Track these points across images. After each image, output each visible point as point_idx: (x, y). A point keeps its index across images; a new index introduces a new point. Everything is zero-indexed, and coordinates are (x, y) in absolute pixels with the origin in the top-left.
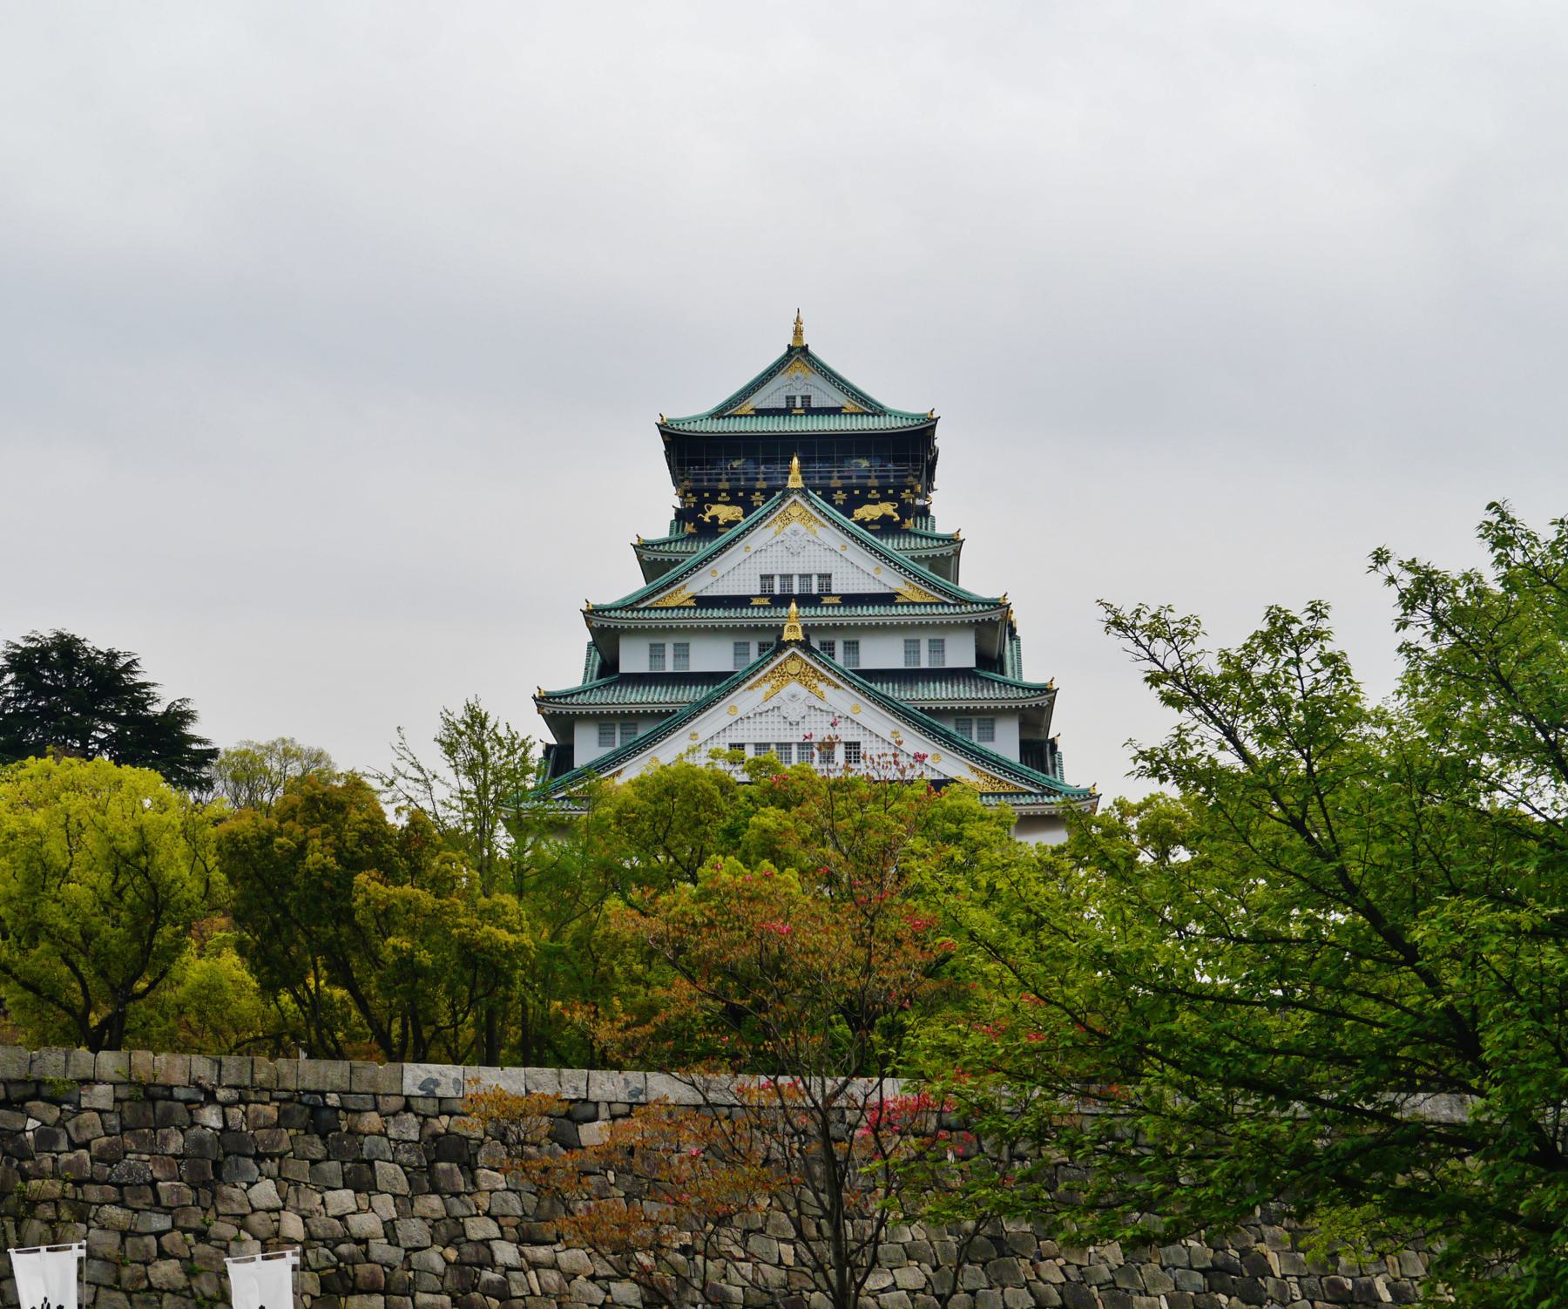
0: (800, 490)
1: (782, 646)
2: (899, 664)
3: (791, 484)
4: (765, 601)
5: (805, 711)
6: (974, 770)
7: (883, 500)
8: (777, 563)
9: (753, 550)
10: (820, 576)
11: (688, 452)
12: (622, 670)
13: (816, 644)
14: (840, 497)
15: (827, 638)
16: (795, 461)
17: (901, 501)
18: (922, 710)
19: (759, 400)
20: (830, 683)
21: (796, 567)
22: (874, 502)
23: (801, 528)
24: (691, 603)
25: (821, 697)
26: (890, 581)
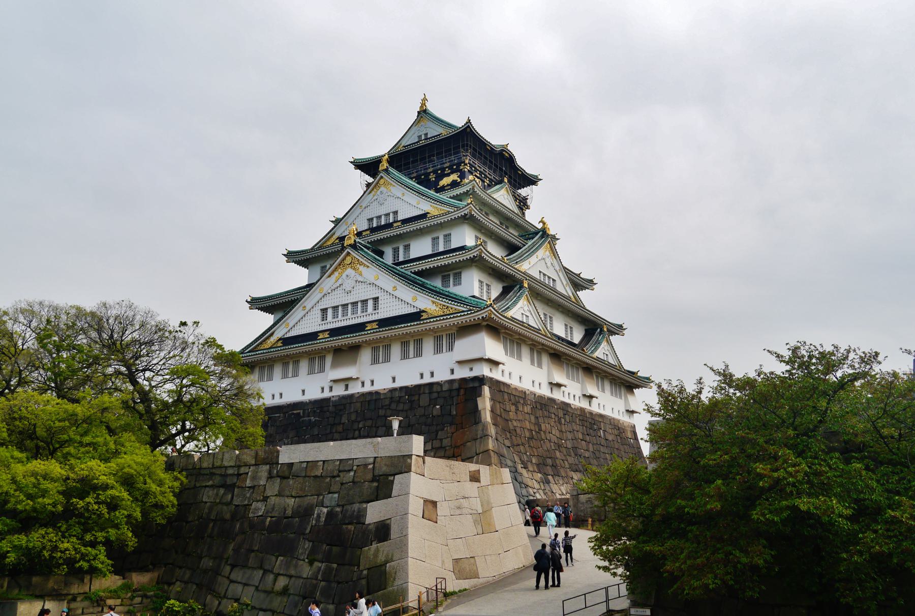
1: (343, 248)
2: (430, 252)
4: (368, 232)
6: (433, 302)
7: (452, 173)
13: (377, 250)
14: (432, 177)
15: (395, 246)
17: (460, 171)
18: (415, 273)
19: (404, 143)
20: (365, 265)
21: (382, 211)
22: (448, 175)
25: (361, 275)
26: (425, 206)
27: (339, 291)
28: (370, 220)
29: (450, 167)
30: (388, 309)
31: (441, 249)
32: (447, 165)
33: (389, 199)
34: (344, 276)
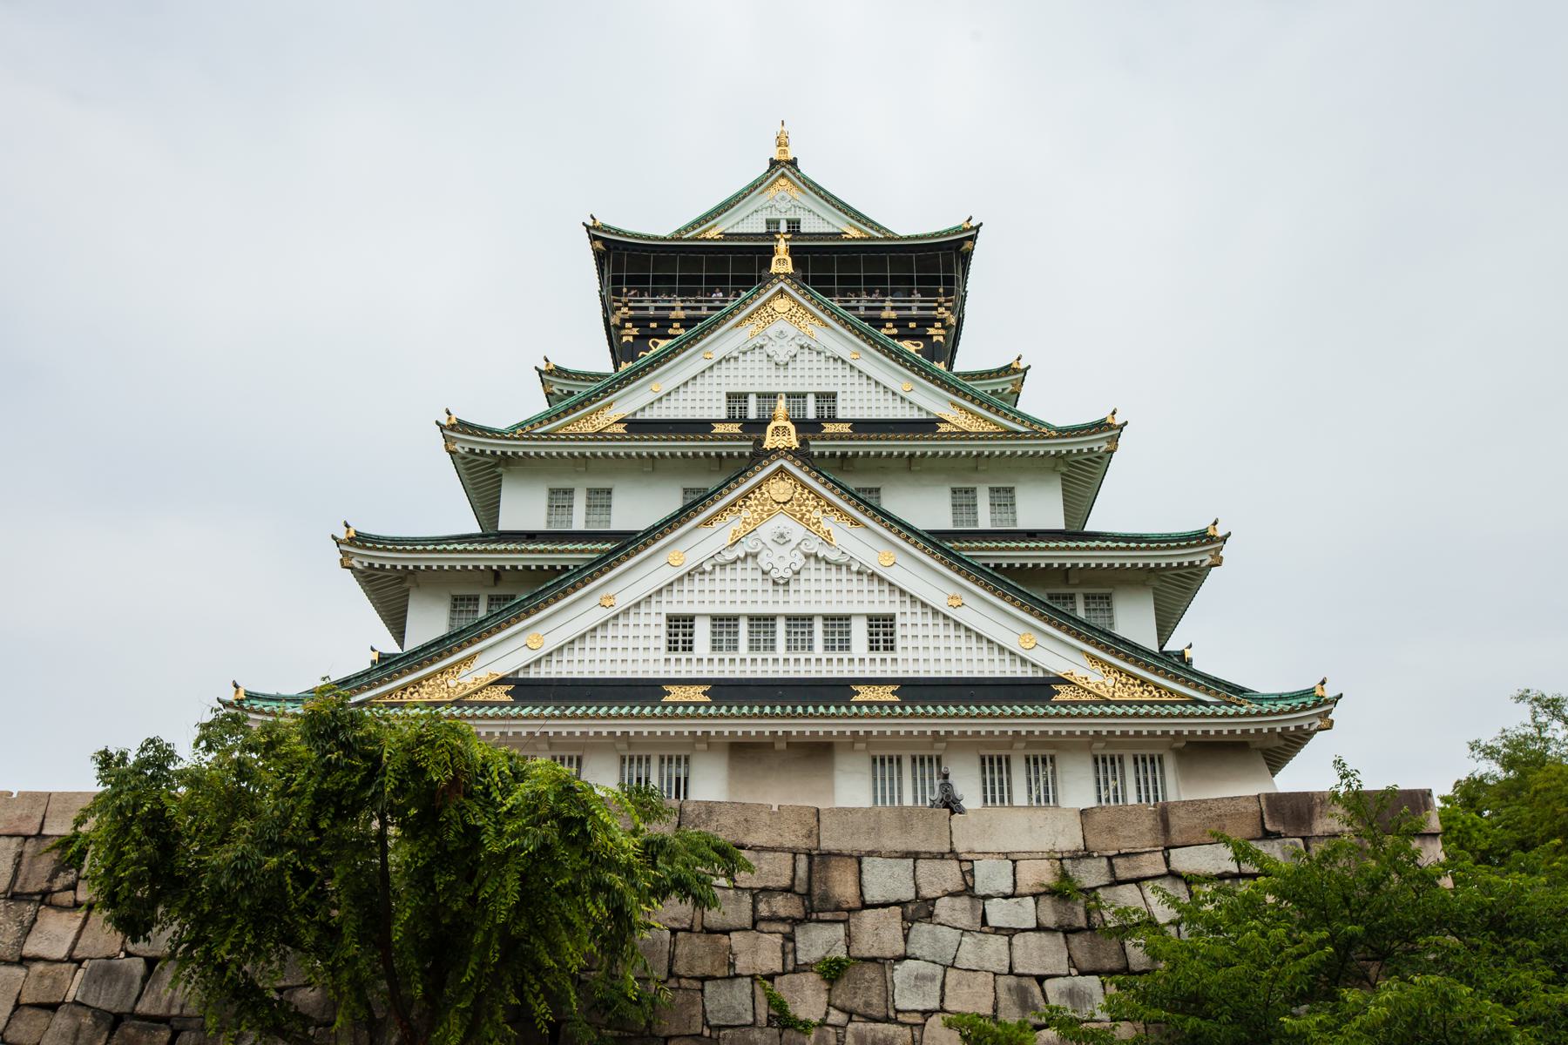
0: (787, 275)
1: (760, 456)
3: (774, 268)
4: (734, 428)
5: (799, 561)
7: (900, 337)
8: (753, 377)
9: (717, 357)
10: (818, 395)
11: (628, 264)
12: (500, 528)
16: (782, 246)
18: (997, 567)
20: (844, 513)
23: (791, 331)
24: (620, 429)
25: (827, 540)
27: (746, 573)
28: (737, 398)
29: (900, 323)
30: (926, 653)
31: (985, 522)
32: (893, 315)
33: (806, 355)
34: (767, 531)
